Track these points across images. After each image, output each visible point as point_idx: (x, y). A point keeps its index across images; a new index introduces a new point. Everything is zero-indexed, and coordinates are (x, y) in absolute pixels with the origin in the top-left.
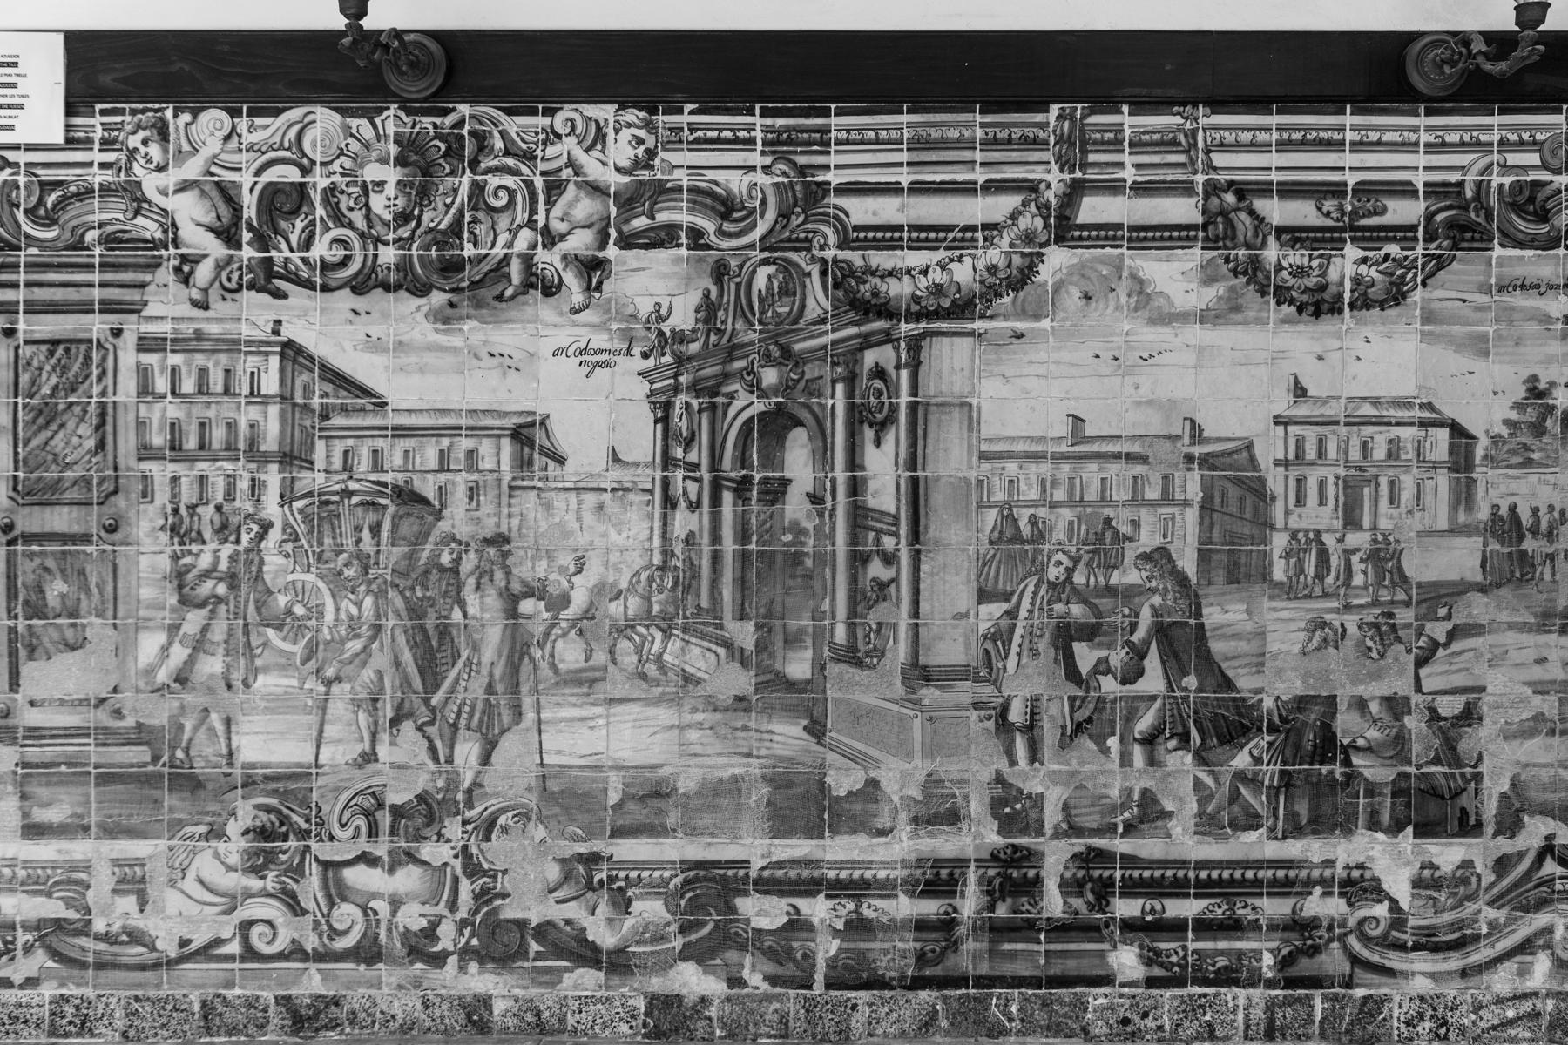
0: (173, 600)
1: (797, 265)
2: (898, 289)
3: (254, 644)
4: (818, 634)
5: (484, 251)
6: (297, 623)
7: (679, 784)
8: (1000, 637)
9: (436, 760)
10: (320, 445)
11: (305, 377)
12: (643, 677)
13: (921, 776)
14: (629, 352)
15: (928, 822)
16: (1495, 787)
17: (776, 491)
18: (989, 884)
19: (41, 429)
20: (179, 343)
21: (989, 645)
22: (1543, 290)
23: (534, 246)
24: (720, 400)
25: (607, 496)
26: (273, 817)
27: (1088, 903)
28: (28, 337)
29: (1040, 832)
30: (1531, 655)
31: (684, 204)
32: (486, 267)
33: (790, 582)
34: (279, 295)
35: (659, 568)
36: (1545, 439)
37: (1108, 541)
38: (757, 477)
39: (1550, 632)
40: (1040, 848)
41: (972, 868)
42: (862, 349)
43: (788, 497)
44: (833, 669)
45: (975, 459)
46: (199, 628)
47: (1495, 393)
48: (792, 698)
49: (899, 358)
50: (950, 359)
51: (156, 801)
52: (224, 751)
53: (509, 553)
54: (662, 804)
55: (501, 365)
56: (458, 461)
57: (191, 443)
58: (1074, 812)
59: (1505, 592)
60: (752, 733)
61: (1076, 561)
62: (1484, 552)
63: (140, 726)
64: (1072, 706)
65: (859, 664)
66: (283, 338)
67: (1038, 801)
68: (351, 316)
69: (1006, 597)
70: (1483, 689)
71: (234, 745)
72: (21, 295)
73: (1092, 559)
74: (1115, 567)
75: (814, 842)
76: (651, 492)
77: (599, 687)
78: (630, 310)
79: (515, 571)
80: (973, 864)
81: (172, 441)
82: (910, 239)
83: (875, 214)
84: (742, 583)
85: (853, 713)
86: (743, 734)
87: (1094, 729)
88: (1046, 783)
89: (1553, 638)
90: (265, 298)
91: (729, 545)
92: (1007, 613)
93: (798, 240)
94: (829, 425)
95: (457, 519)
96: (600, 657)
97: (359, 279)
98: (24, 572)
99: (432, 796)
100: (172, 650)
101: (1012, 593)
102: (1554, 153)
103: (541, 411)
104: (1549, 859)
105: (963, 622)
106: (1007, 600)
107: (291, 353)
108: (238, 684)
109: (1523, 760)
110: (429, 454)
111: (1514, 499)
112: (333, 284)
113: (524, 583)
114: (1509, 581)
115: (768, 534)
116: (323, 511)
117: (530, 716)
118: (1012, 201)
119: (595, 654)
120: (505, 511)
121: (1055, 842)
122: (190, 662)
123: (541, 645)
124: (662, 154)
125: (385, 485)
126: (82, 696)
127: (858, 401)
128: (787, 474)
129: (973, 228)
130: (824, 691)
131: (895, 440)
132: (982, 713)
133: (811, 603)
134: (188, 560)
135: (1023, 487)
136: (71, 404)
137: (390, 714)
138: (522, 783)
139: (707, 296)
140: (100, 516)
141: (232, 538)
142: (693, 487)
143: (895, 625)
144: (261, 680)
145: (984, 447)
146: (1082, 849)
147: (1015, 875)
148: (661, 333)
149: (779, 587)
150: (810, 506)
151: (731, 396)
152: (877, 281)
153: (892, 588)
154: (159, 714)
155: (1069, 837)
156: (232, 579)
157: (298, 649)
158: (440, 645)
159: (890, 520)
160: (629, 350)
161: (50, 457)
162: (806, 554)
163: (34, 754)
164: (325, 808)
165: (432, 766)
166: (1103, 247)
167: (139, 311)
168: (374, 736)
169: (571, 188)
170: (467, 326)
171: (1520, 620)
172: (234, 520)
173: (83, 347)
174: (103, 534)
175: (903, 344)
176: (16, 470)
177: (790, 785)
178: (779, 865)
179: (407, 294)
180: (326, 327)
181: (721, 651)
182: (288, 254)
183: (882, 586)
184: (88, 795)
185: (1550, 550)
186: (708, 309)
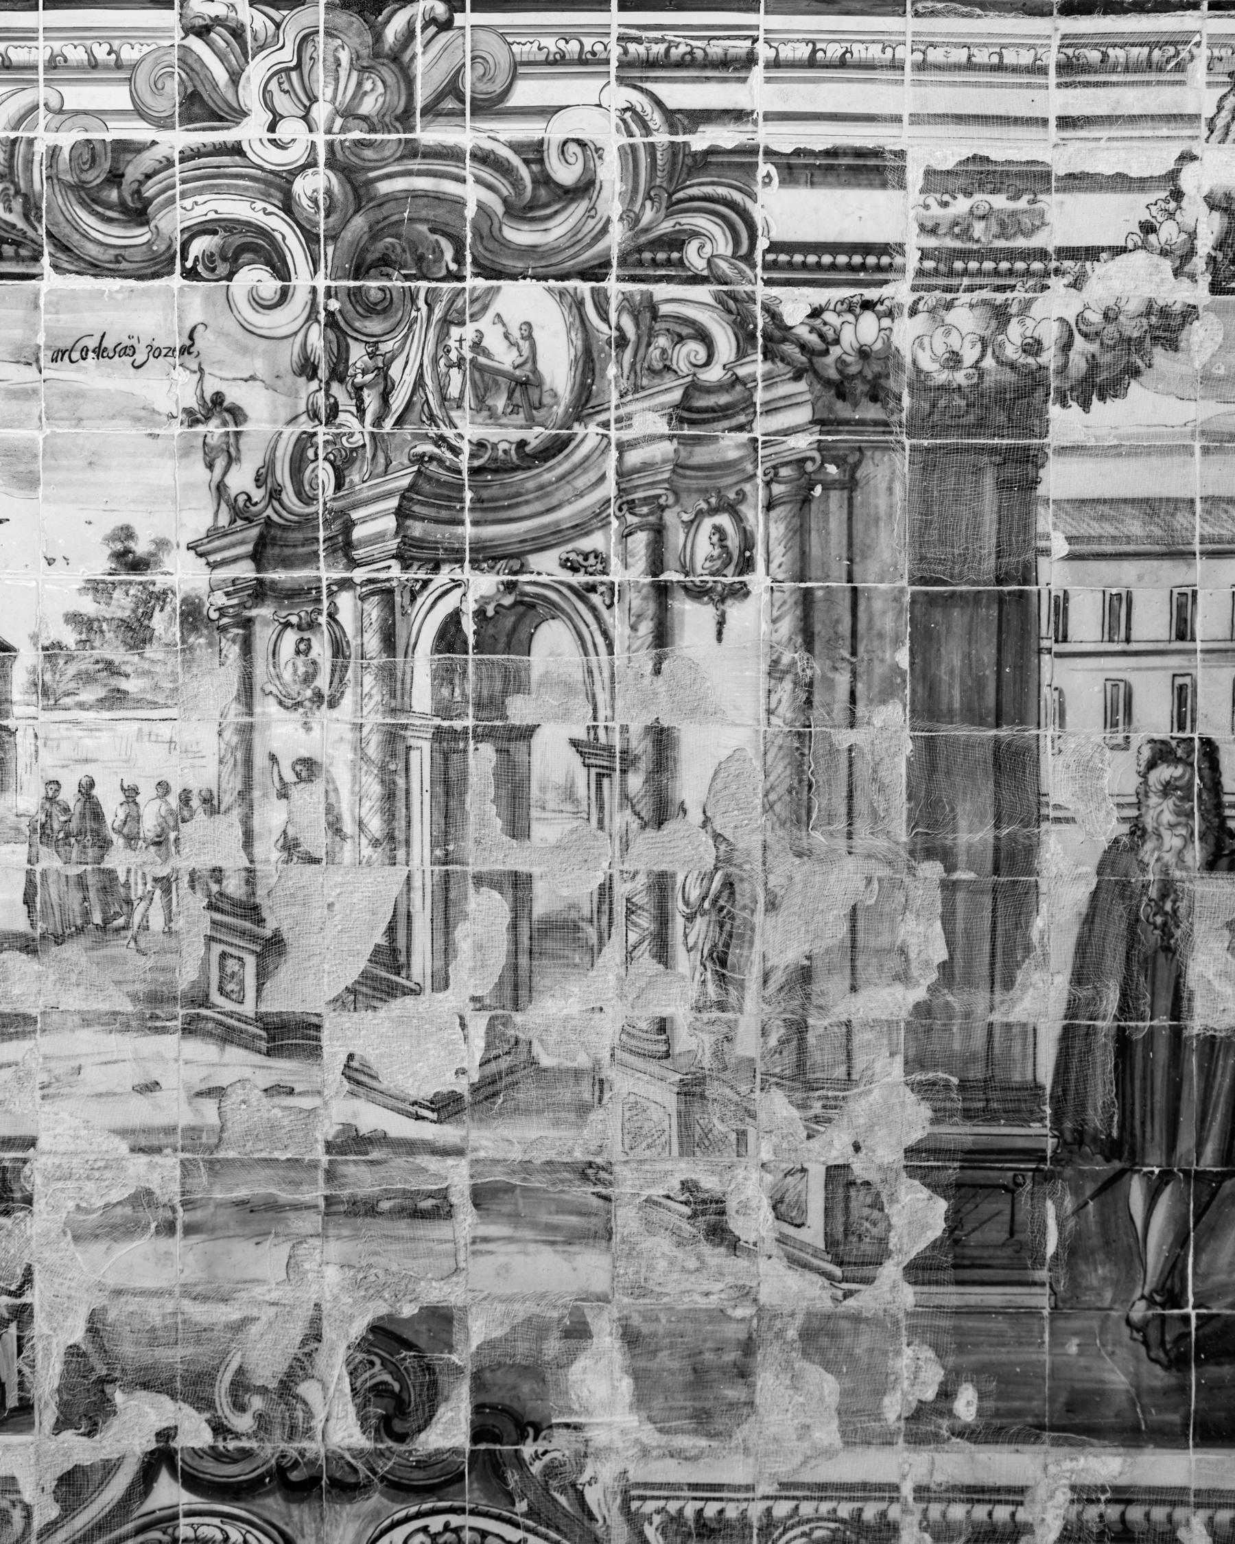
16: (57, 1333)
22: (140, 357)
30: (132, 1075)
36: (151, 652)
39: (163, 1031)
47: (50, 562)
59: (73, 951)
62: (30, 873)
70: (31, 1143)
89: (170, 1043)
102: (157, 88)
104: (164, 1476)
109: (112, 1281)
111: (90, 770)
114: (80, 930)
171: (105, 1007)
185: (163, 872)
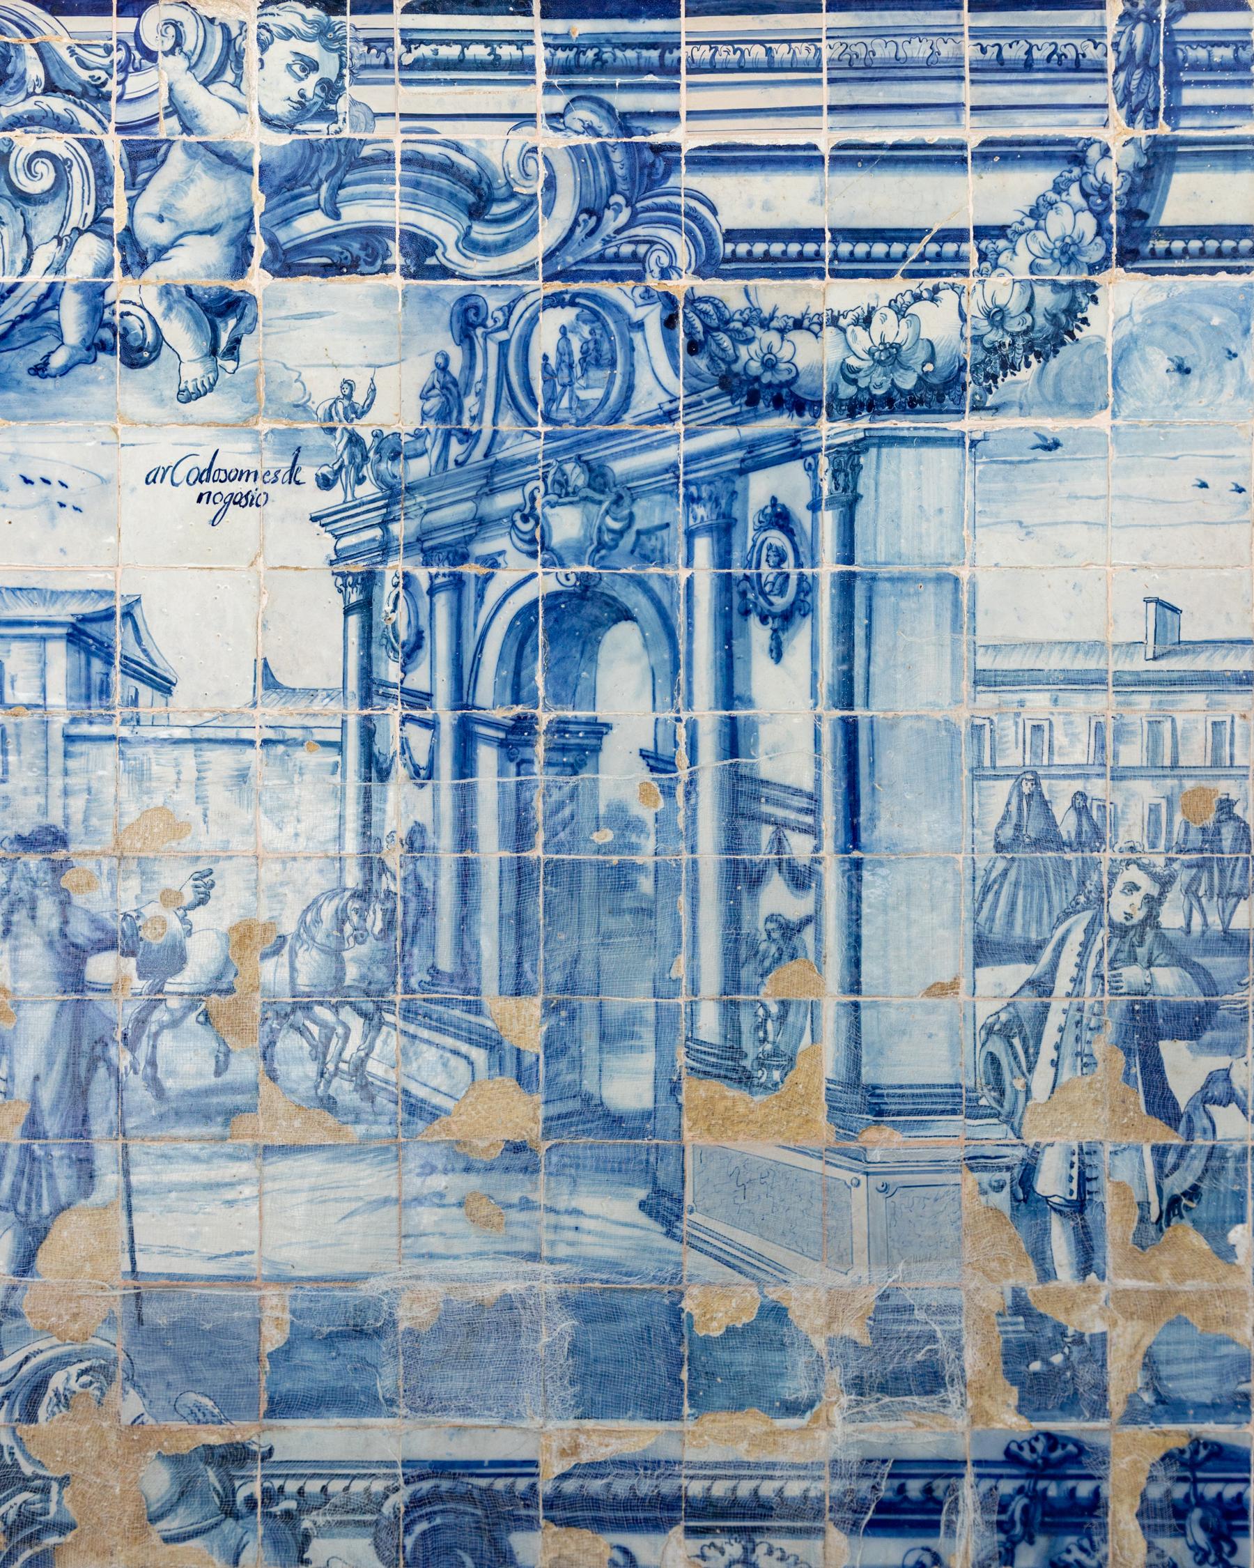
2: (814, 357)
4: (664, 1023)
7: (400, 1313)
8: (1018, 1032)
13: (868, 1298)
14: (293, 476)
15: (883, 1389)
17: (580, 746)
18: (1003, 1508)
21: (997, 1046)
23: (107, 270)
24: (470, 570)
25: (253, 756)
27: (1195, 1548)
29: (1099, 1410)
31: (397, 187)
33: (610, 923)
35: (357, 895)
37: (1227, 844)
38: (545, 718)
40: (1101, 1440)
41: (969, 1479)
42: (743, 472)
43: (603, 756)
44: (695, 1091)
45: (966, 685)
48: (617, 1146)
49: (817, 489)
50: (917, 491)
55: (46, 501)
58: (1165, 1370)
61: (1165, 883)
64: (1160, 1166)
65: (745, 1080)
67: (1094, 1349)
69: (1030, 953)
73: (1195, 880)
74: (1240, 895)
75: (661, 1426)
76: (339, 746)
77: (244, 1123)
78: (295, 395)
79: (78, 899)
80: (970, 1471)
82: (835, 256)
83: (767, 207)
84: (518, 923)
85: (734, 1175)
86: (523, 1216)
87: (1202, 1209)
88: (1109, 1314)
91: (491, 851)
92: (1031, 983)
93: (617, 258)
94: (681, 618)
96: (245, 1067)
101: (1040, 946)
103: (125, 589)
105: (947, 1002)
106: (1031, 959)
113: (96, 923)
115: (566, 829)
117: (109, 1180)
118: (1037, 180)
119: (233, 1059)
121: (1129, 1429)
124: (353, 90)
127: (737, 571)
128: (602, 714)
129: (958, 235)
130: (679, 1134)
131: (813, 640)
132: (986, 1177)
133: (652, 964)
135: (1060, 739)
139: (443, 368)
142: (420, 739)
143: (814, 1007)
145: (984, 662)
146: (1184, 1443)
147: (1053, 1490)
148: (354, 440)
149: (589, 931)
150: (647, 776)
151: (492, 562)
152: (772, 337)
153: (808, 933)
155: (1156, 1419)
159: (804, 803)
160: (293, 471)
162: (641, 868)
166: (1213, 271)
169: (177, 155)
175: (824, 462)
177: (614, 1315)
178: (595, 1469)
181: (479, 1055)
183: (789, 930)
186: (447, 393)
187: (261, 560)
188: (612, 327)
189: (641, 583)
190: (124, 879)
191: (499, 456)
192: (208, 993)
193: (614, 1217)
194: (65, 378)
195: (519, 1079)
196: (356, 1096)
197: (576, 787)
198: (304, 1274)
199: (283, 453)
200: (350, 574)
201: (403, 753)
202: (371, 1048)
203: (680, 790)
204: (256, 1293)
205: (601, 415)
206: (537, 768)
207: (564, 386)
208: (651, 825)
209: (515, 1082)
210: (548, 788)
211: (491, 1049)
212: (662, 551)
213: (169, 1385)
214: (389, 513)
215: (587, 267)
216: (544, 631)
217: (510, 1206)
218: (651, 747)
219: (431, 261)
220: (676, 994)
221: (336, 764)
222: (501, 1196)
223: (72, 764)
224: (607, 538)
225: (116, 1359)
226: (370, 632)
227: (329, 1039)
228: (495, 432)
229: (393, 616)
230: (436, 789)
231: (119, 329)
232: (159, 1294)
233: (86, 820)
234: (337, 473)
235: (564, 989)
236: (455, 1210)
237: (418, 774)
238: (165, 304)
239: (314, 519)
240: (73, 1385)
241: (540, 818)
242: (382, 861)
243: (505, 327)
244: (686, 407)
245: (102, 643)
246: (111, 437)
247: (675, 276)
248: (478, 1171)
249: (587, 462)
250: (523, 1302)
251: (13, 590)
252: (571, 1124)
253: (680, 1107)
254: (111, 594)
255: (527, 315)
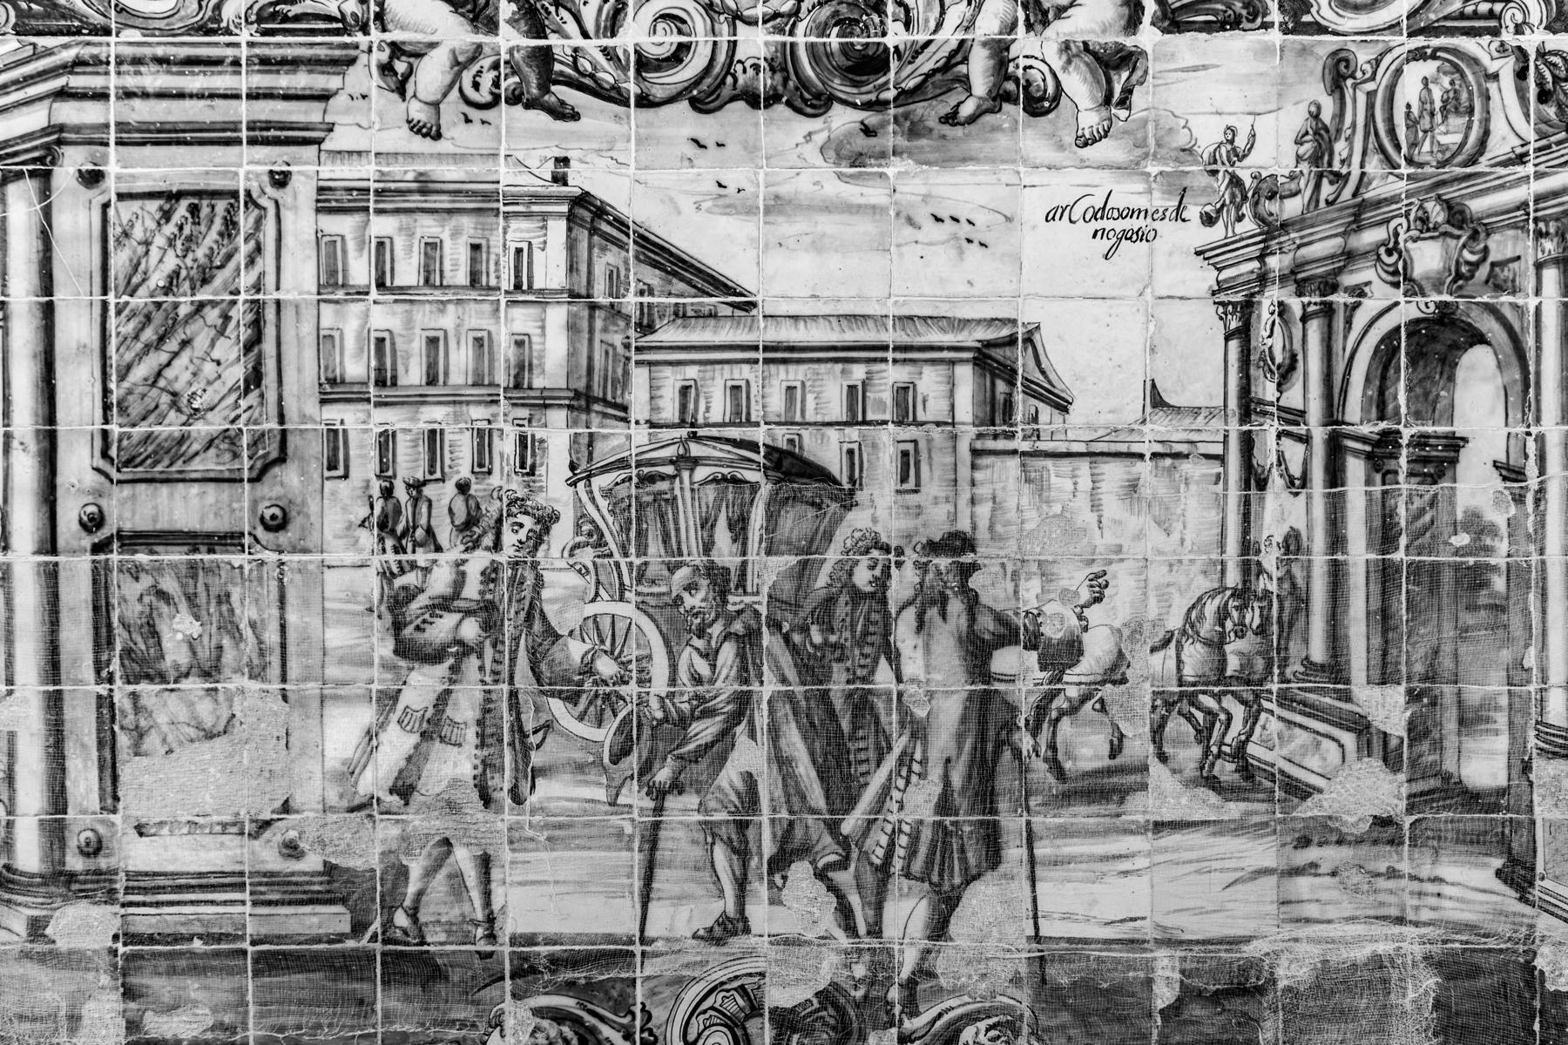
0: (384, 648)
1: (1474, 61)
3: (529, 726)
5: (922, 38)
6: (602, 689)
7: (1280, 972)
9: (850, 929)
10: (639, 377)
11: (612, 257)
12: (1212, 783)
14: (1179, 214)
17: (1440, 459)
19: (148, 348)
20: (388, 197)
23: (1012, 27)
24: (1340, 298)
25: (1144, 468)
26: (566, 1030)
28: (124, 188)
32: (926, 63)
33: (1468, 619)
34: (563, 113)
35: (1236, 594)
38: (1407, 434)
43: (1460, 467)
44: (1544, 770)
46: (432, 698)
48: (1474, 820)
51: (361, 1002)
52: (480, 915)
53: (974, 567)
54: (1251, 1008)
55: (955, 237)
56: (881, 405)
57: (413, 375)
60: (1404, 882)
63: (330, 870)
66: (572, 190)
68: (691, 150)
71: (497, 903)
72: (111, 112)
76: (1221, 459)
78: (1182, 139)
79: (985, 599)
81: (380, 370)
84: (1383, 618)
86: (1391, 884)
90: (539, 118)
91: (1359, 554)
93: (1476, 16)
94: (1530, 341)
95: (880, 509)
96: (1139, 746)
97: (704, 87)
98: (124, 599)
99: (846, 994)
100: (383, 737)
103: (1028, 314)
107: (587, 215)
108: (504, 797)
110: (828, 393)
112: (659, 93)
113: (1000, 618)
115: (1425, 536)
116: (647, 494)
117: (1014, 853)
119: (1126, 742)
120: (965, 495)
122: (415, 760)
123: (1035, 731)
125: (753, 446)
126: (227, 818)
128: (1459, 429)
133: (1506, 655)
134: (411, 579)
136: (201, 306)
137: (768, 848)
138: (1003, 971)
140: (255, 503)
141: (488, 540)
142: (1294, 452)
144: (548, 791)
148: (1235, 182)
150: (1499, 484)
151: (1359, 291)
154: (366, 850)
156: (487, 612)
157: (605, 735)
158: (855, 728)
161: (165, 399)
162: (1495, 569)
163: (146, 920)
164: (659, 1015)
165: (844, 941)
167: (319, 142)
168: (742, 884)
170: (894, 168)
172: (492, 509)
173: (221, 206)
174: (260, 532)
176: (106, 422)
179: (788, 112)
180: (647, 169)
181: (1348, 739)
182: (579, 41)
184: (242, 992)
186: (1320, 139)
187: (1148, 290)
188: (1471, 78)
189: (1492, 310)
190: (1027, 580)
191: (1366, 196)
192: (1103, 682)
193: (1472, 884)
194: (972, 127)
195: (1385, 760)
196: (1237, 776)
197: (1435, 496)
198: (1194, 937)
199: (1170, 193)
200: (1230, 303)
201: (1279, 464)
202: (1250, 734)
203: (1530, 498)
204: (1148, 955)
205: (1459, 159)
206: (1401, 477)
207: (1425, 132)
208: (1504, 530)
209: (1381, 763)
210: (1410, 496)
211: (1359, 733)
212: (1513, 281)
213: (1070, 1038)
214: (1266, 248)
215: (1449, 24)
216: (1407, 354)
217: (1378, 875)
218: (1504, 460)
219: (1306, 18)
220: (1529, 682)
221: (1218, 476)
222: (1371, 866)
223: (979, 476)
224: (1464, 269)
225: (1022, 1016)
226: (1249, 355)
227: (1213, 725)
228: (1363, 174)
229: (1269, 342)
230: (1309, 497)
231: (1022, 82)
232: (1061, 956)
233: (991, 528)
234: (1219, 211)
235: (1425, 678)
236: (1328, 879)
237: (1293, 484)
238: (1064, 58)
239: (1198, 253)
240: (982, 1038)
241: (1403, 524)
242: (1259, 564)
243: (1373, 78)
244: (1536, 150)
245: (1005, 366)
246: (1015, 180)
247: (1528, 31)
248: (1350, 843)
249: (1447, 201)
250: (1392, 961)
251: (924, 319)
252: (1433, 800)
253: (1531, 784)
254: (1014, 322)
255: (1393, 67)
